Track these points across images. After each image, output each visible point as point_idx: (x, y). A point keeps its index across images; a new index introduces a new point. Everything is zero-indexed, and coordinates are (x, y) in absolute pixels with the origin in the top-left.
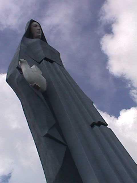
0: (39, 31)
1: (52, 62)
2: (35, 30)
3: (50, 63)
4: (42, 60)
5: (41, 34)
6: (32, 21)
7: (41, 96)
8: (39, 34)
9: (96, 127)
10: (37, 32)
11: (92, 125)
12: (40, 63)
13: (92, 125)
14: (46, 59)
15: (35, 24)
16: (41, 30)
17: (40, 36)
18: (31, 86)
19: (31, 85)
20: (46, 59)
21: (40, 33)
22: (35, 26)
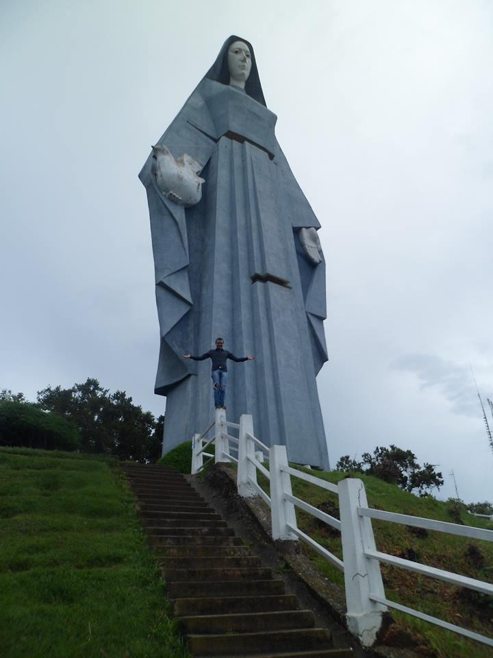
0: (242, 64)
1: (241, 139)
2: (235, 59)
3: (236, 144)
4: (219, 139)
5: (247, 73)
6: (233, 39)
7: (179, 214)
8: (244, 71)
9: (259, 284)
10: (239, 66)
11: (256, 278)
12: (216, 141)
13: (256, 278)
14: (231, 135)
15: (238, 45)
16: (249, 61)
17: (243, 74)
18: (165, 195)
19: (164, 193)
20: (231, 135)
21: (244, 69)
22: (236, 52)
